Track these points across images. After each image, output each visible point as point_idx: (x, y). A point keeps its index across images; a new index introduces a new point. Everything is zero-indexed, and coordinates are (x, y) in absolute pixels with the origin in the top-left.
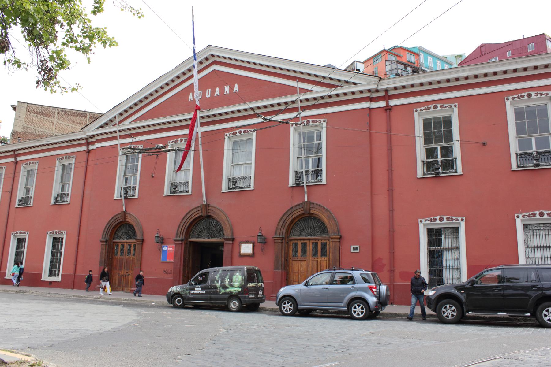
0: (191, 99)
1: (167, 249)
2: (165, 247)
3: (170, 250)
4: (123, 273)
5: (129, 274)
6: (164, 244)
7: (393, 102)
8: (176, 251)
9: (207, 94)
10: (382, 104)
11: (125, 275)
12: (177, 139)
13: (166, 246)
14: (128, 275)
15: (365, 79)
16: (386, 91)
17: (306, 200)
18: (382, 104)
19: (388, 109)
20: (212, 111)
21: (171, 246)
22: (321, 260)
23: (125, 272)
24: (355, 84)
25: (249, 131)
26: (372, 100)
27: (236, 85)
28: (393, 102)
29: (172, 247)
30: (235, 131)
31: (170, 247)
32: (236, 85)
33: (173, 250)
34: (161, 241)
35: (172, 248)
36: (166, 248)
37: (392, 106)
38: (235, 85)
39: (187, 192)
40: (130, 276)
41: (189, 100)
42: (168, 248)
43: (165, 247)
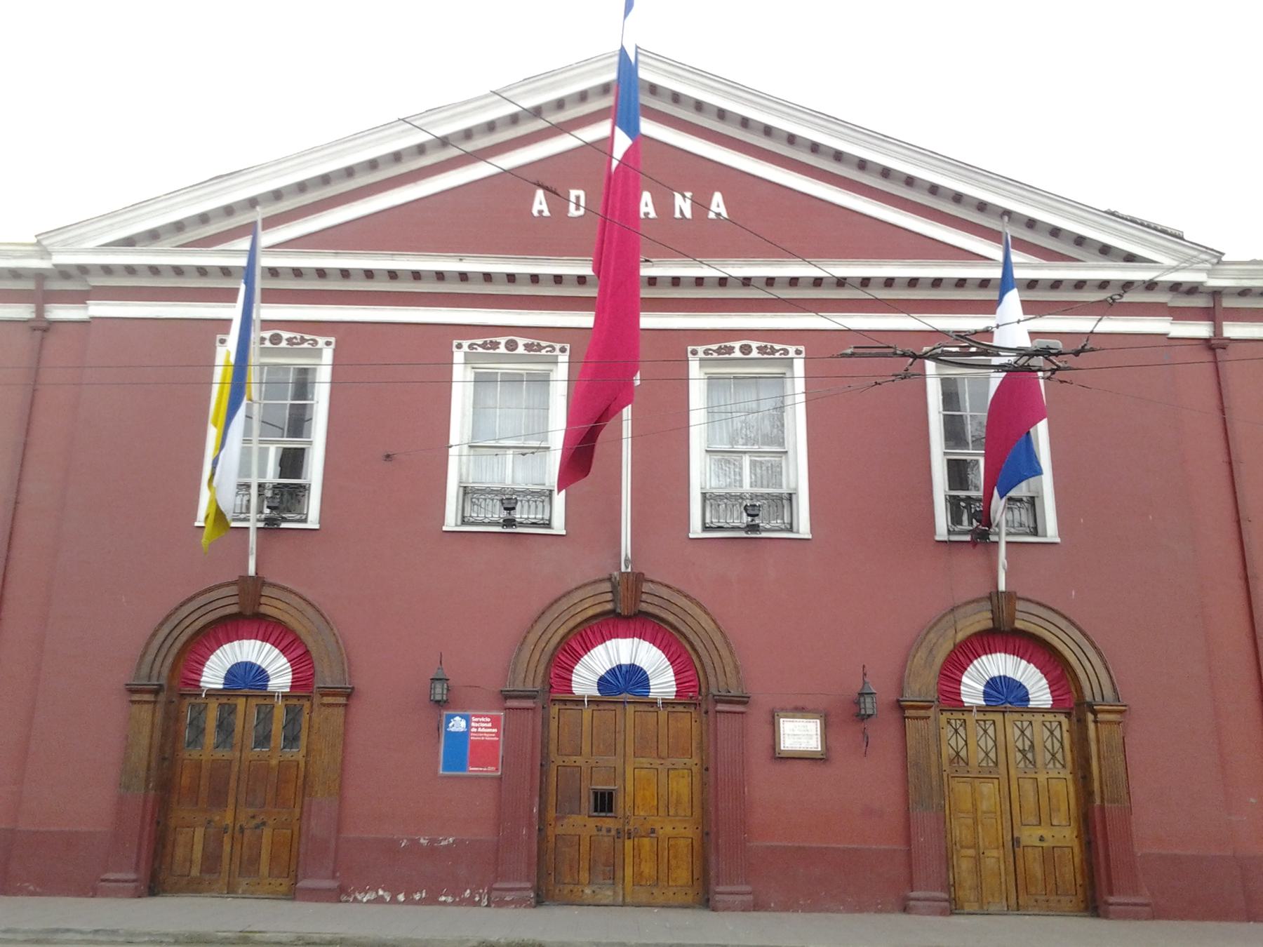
0: (541, 212)
1: (468, 726)
2: (457, 718)
3: (480, 730)
4: (229, 820)
5: (264, 824)
6: (455, 709)
7: (1233, 330)
8: (509, 733)
10: (1201, 330)
12: (494, 339)
14: (257, 827)
15: (1175, 251)
16: (1217, 293)
17: (1002, 587)
18: (1201, 330)
19: (1213, 346)
20: (653, 266)
21: (484, 716)
22: (1047, 779)
23: (242, 819)
24: (1130, 258)
25: (778, 351)
26: (1179, 314)
27: (717, 198)
28: (1233, 330)
29: (488, 720)
30: (728, 344)
31: (483, 719)
32: (717, 198)
33: (495, 730)
35: (490, 725)
36: (463, 723)
37: (1229, 339)
38: (712, 195)
39: (548, 525)
40: (267, 832)
41: (535, 213)
42: (473, 724)
43: (457, 718)
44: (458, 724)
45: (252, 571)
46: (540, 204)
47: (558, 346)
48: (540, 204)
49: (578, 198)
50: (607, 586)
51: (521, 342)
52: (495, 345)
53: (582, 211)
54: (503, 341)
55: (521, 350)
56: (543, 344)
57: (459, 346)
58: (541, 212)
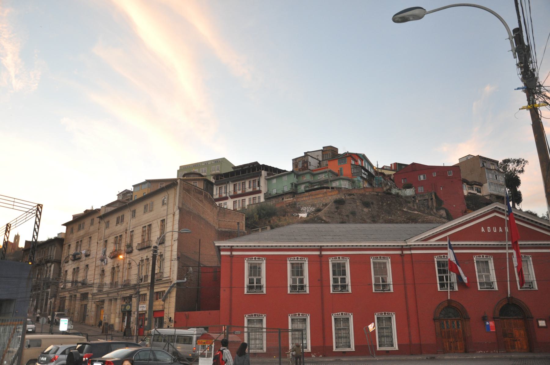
1: (489, 323)
5: (457, 341)
9: (490, 229)
11: (454, 342)
13: (489, 322)
14: (456, 342)
34: (484, 319)
44: (488, 323)
45: (449, 298)
46: (483, 230)
47: (491, 256)
48: (483, 230)
49: (489, 228)
50: (507, 299)
51: (485, 256)
52: (480, 256)
53: (490, 231)
54: (481, 255)
55: (485, 257)
56: (488, 256)
57: (474, 257)
58: (483, 231)
